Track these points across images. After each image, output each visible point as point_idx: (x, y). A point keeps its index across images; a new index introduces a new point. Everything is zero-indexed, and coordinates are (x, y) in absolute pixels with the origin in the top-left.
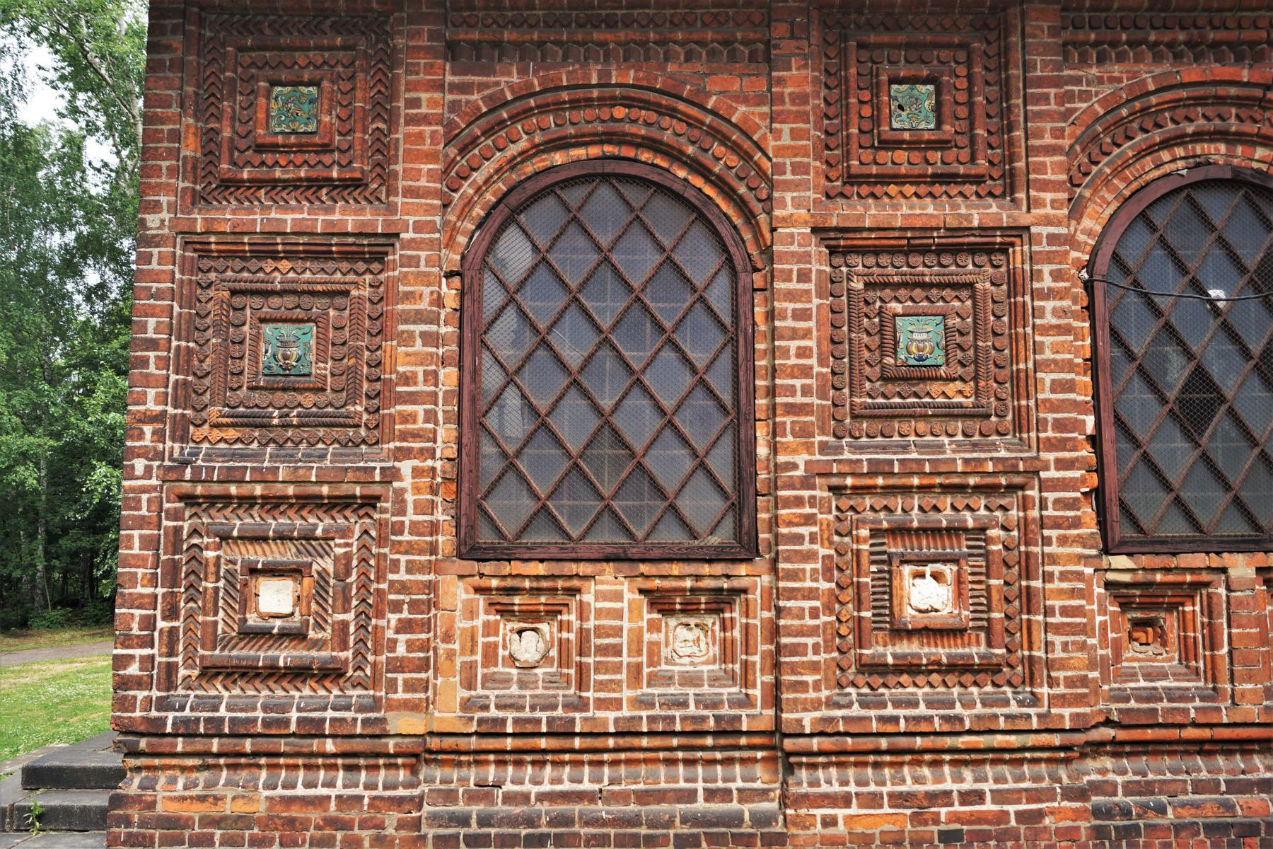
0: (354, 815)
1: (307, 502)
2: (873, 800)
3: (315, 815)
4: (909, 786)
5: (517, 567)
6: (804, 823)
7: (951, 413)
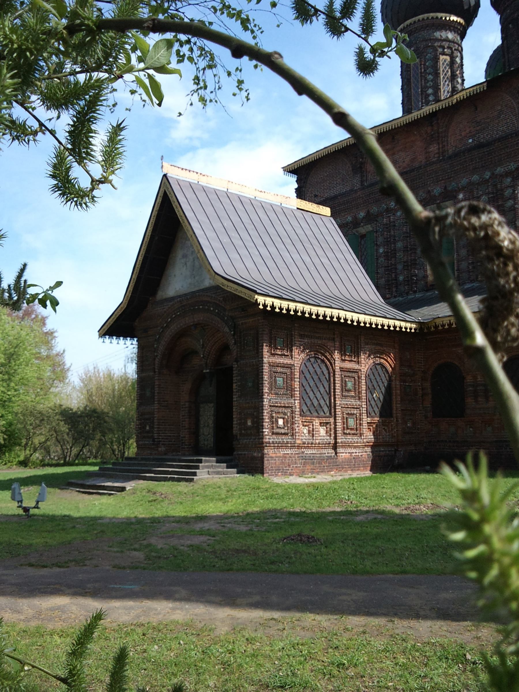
0: (292, 456)
1: (284, 407)
2: (346, 453)
3: (288, 456)
4: (349, 451)
5: (307, 418)
6: (339, 456)
7: (352, 397)
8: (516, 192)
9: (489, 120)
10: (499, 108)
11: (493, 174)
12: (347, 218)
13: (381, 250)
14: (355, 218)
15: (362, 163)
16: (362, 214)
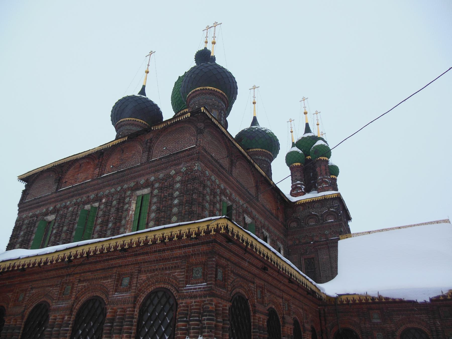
8: (131, 199)
9: (127, 158)
10: (134, 152)
11: (122, 188)
12: (43, 210)
13: (54, 232)
14: (47, 210)
15: (60, 177)
16: (51, 208)
